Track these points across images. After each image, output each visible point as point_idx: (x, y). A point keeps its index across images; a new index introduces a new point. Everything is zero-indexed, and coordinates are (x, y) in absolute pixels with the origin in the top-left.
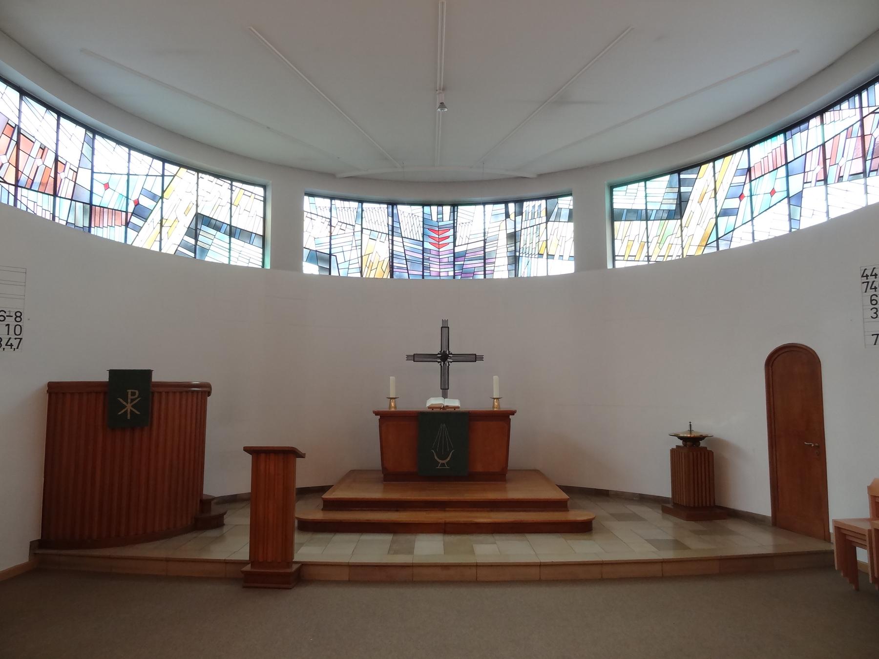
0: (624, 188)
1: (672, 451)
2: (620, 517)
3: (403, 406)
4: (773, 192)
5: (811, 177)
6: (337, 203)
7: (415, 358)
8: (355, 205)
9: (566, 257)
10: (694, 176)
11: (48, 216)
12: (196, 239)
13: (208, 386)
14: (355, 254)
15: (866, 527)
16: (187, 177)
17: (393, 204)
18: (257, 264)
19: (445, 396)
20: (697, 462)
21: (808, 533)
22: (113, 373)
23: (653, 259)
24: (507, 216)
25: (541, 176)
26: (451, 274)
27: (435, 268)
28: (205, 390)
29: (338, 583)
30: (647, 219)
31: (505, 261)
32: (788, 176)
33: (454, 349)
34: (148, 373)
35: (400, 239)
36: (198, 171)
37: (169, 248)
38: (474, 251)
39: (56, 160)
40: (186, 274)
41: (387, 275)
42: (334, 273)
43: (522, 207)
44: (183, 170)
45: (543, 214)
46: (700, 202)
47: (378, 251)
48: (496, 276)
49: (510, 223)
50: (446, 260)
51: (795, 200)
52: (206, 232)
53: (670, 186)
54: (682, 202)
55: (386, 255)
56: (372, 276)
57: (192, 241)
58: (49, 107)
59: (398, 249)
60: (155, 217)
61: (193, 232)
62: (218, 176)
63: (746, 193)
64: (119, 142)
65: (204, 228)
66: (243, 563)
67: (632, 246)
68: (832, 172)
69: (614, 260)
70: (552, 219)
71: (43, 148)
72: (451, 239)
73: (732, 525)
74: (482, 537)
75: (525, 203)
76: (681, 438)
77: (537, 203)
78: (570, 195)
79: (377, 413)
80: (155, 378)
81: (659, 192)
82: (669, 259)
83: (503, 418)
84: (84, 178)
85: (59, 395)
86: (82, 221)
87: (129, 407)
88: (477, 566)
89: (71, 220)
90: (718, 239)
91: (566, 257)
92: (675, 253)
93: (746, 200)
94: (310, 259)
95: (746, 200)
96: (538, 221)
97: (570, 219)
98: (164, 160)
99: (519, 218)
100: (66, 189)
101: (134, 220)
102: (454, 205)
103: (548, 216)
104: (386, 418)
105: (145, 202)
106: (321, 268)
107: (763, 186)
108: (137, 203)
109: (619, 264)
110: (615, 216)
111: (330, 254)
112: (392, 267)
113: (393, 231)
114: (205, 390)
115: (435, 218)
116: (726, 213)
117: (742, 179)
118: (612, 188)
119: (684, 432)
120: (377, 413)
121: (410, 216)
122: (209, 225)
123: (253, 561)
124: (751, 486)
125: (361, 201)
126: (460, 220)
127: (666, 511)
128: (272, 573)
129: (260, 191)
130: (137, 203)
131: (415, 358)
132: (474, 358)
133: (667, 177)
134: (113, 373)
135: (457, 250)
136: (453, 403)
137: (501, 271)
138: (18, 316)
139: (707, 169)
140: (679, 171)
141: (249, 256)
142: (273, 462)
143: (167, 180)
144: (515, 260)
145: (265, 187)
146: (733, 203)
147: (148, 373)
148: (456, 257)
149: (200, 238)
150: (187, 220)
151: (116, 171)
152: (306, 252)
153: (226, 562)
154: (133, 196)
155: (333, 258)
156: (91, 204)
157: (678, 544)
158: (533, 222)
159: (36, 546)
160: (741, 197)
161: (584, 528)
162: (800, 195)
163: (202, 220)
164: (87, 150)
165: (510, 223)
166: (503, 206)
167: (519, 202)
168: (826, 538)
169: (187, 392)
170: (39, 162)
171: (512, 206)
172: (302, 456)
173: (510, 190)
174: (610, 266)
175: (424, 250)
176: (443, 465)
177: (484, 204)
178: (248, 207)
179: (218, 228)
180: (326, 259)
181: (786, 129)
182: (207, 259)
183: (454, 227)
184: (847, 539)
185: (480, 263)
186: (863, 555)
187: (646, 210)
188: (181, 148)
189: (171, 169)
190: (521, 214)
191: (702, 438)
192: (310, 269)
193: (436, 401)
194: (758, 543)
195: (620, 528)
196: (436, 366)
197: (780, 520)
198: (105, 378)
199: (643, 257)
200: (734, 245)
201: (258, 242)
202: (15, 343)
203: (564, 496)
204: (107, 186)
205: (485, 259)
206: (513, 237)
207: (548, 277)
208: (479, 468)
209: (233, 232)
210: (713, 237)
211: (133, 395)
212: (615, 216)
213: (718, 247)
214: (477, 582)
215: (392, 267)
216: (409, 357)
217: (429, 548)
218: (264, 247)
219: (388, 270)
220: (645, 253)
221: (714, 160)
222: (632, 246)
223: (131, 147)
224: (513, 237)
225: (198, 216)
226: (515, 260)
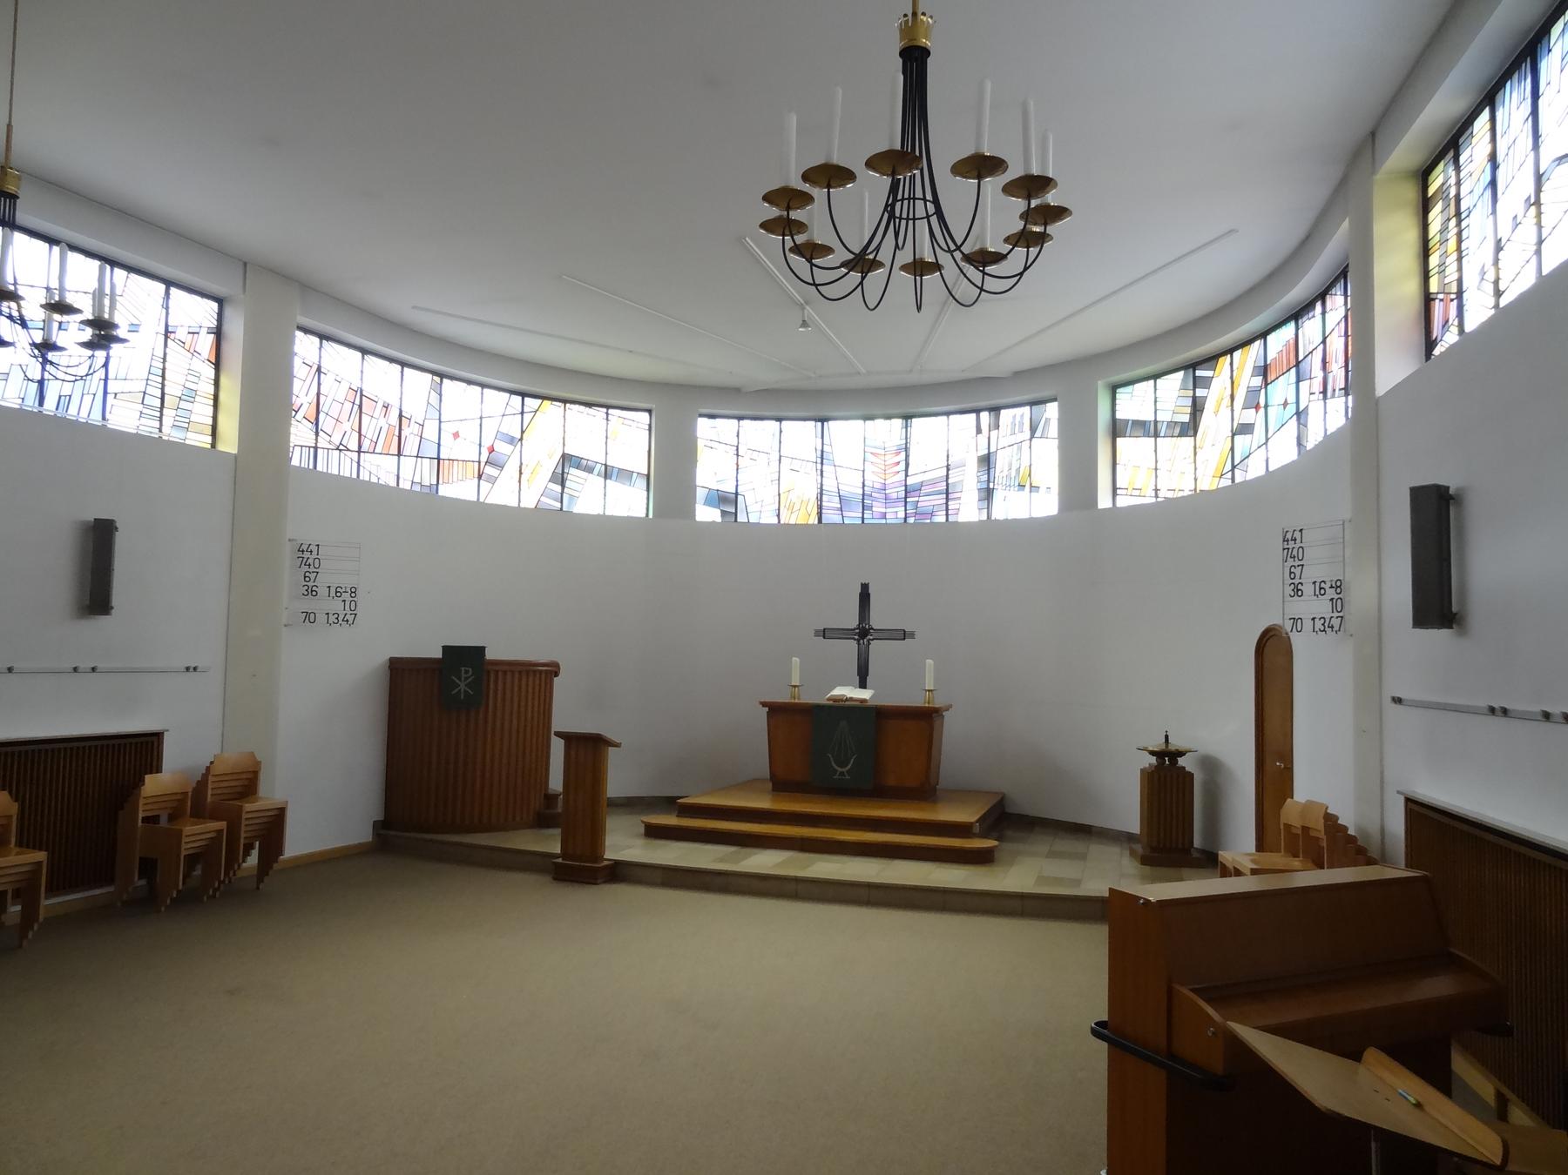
0: (1129, 389)
2: (1052, 855)
3: (808, 698)
4: (1285, 404)
6: (744, 423)
7: (825, 633)
8: (774, 424)
10: (1208, 373)
11: (393, 483)
12: (563, 486)
13: (557, 665)
16: (551, 410)
18: (643, 515)
22: (446, 649)
23: (1161, 494)
24: (979, 431)
25: (1018, 375)
26: (901, 514)
27: (878, 508)
28: (553, 670)
30: (1156, 435)
31: (975, 495)
32: (1298, 381)
34: (481, 650)
36: (565, 401)
37: (529, 502)
38: (934, 482)
39: (401, 416)
40: (551, 530)
41: (813, 520)
42: (742, 518)
44: (547, 403)
48: (962, 518)
49: (983, 438)
50: (894, 496)
51: (1300, 415)
52: (574, 474)
53: (1184, 387)
54: (1197, 408)
56: (792, 522)
57: (558, 488)
58: (391, 360)
59: (829, 485)
61: (560, 479)
63: (1262, 403)
64: (470, 382)
65: (573, 471)
66: (556, 856)
69: (1114, 494)
70: (1038, 434)
71: (386, 407)
72: (902, 466)
76: (1152, 753)
78: (1055, 400)
79: (764, 704)
80: (489, 655)
81: (1170, 393)
82: (1181, 494)
83: (926, 718)
84: (431, 432)
85: (399, 670)
86: (428, 478)
87: (462, 686)
89: (417, 480)
90: (1234, 467)
92: (1184, 487)
94: (708, 502)
95: (1262, 411)
96: (1020, 437)
98: (523, 395)
100: (410, 447)
101: (489, 470)
102: (907, 417)
103: (1033, 430)
104: (775, 711)
105: (502, 448)
106: (724, 513)
108: (491, 450)
109: (1122, 502)
111: (737, 494)
112: (820, 507)
114: (553, 670)
116: (1246, 429)
118: (1114, 389)
119: (1157, 743)
120: (764, 704)
122: (578, 467)
123: (564, 855)
125: (780, 420)
128: (583, 868)
130: (491, 450)
131: (825, 633)
132: (904, 635)
133: (1182, 373)
134: (446, 649)
136: (865, 694)
137: (968, 510)
138: (354, 591)
139: (1224, 361)
140: (1192, 366)
141: (631, 502)
142: (588, 750)
143: (527, 417)
144: (987, 494)
145: (650, 411)
146: (1249, 416)
147: (481, 650)
148: (908, 491)
149: (568, 484)
151: (471, 412)
152: (701, 494)
154: (486, 443)
155: (740, 498)
156: (439, 459)
158: (1013, 439)
159: (378, 826)
160: (1257, 407)
161: (982, 858)
164: (434, 397)
165: (983, 438)
166: (973, 416)
167: (995, 410)
169: (528, 672)
170: (382, 422)
171: (985, 416)
172: (617, 745)
173: (977, 394)
174: (1104, 502)
176: (842, 774)
177: (948, 414)
178: (627, 437)
179: (590, 470)
180: (727, 501)
181: (1297, 314)
182: (576, 510)
183: (906, 449)
185: (941, 499)
187: (1156, 422)
188: (539, 381)
189: (531, 403)
190: (997, 427)
191: (1181, 754)
192: (706, 514)
196: (852, 645)
198: (439, 655)
200: (1251, 476)
202: (351, 618)
204: (456, 435)
205: (947, 493)
206: (987, 461)
207: (1032, 520)
208: (891, 781)
209: (607, 473)
210: (1228, 466)
211: (467, 673)
212: (1117, 429)
213: (1233, 479)
215: (820, 507)
216: (817, 633)
219: (815, 511)
221: (1230, 351)
222: (1146, 473)
223: (483, 386)
224: (987, 461)
225: (566, 458)
226: (987, 494)
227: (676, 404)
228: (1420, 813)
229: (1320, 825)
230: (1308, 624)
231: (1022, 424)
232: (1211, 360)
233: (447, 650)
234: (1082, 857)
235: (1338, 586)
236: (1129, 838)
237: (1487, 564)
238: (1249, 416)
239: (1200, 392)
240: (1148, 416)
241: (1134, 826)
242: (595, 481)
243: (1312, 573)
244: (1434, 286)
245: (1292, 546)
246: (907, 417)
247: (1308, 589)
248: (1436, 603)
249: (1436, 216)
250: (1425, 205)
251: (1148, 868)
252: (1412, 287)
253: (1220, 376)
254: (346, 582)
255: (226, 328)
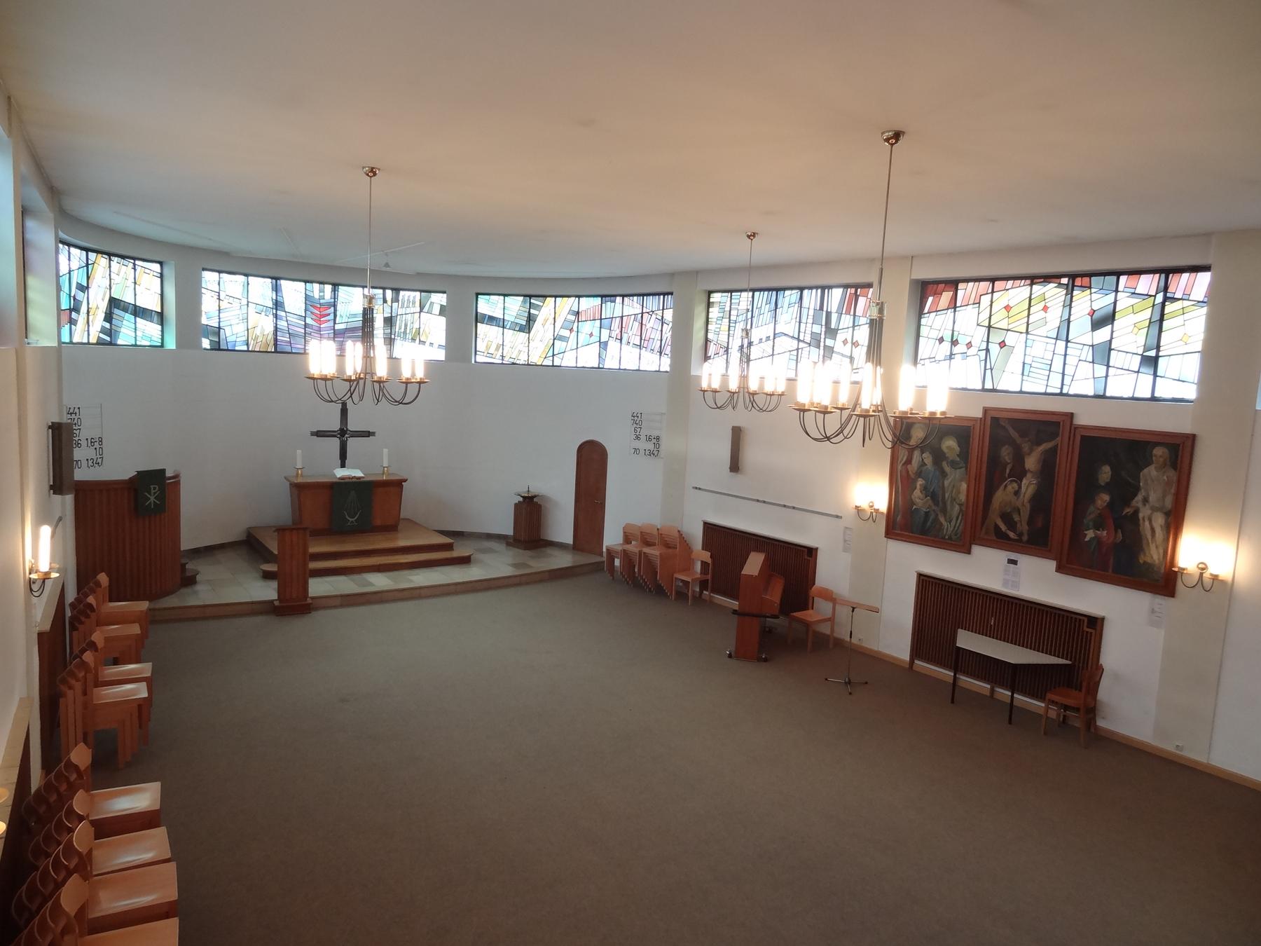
1: (516, 505)
2: (485, 551)
4: (591, 335)
5: (614, 334)
7: (319, 434)
9: (436, 345)
14: (242, 327)
15: (620, 548)
17: (277, 279)
19: (343, 465)
20: (530, 511)
21: (591, 552)
24: (385, 301)
25: (418, 274)
29: (335, 607)
33: (352, 426)
34: (163, 471)
35: (283, 314)
43: (398, 295)
45: (418, 304)
46: (543, 325)
47: (264, 326)
51: (603, 345)
54: (531, 319)
55: (272, 329)
57: (107, 325)
59: (282, 324)
60: (84, 309)
62: (123, 257)
63: (575, 328)
65: (116, 311)
66: (272, 602)
67: (490, 344)
68: (625, 337)
70: (426, 309)
72: (331, 317)
73: (549, 551)
74: (417, 571)
75: (402, 293)
77: (412, 294)
81: (514, 307)
83: (398, 484)
87: (152, 499)
88: (421, 588)
91: (436, 345)
92: (522, 359)
93: (574, 334)
95: (574, 334)
96: (412, 310)
97: (440, 314)
99: (395, 305)
101: (74, 315)
102: (335, 286)
105: (80, 296)
107: (587, 327)
109: (480, 359)
110: (479, 318)
111: (219, 328)
112: (276, 340)
113: (278, 305)
115: (317, 296)
116: (561, 338)
117: (573, 318)
118: (477, 294)
119: (523, 490)
121: (294, 293)
124: (562, 527)
125: (246, 275)
126: (340, 299)
127: (508, 544)
128: (294, 604)
129: (156, 267)
131: (319, 434)
132: (368, 434)
135: (337, 327)
139: (550, 301)
140: (530, 296)
145: (161, 263)
146: (565, 333)
147: (163, 471)
150: (104, 305)
153: (252, 603)
157: (515, 566)
160: (571, 330)
161: (465, 561)
162: (606, 343)
163: (114, 303)
166: (381, 291)
167: (396, 290)
168: (601, 554)
171: (389, 292)
175: (306, 326)
179: (125, 310)
183: (335, 306)
184: (611, 554)
186: (617, 562)
189: (92, 256)
190: (397, 301)
193: (340, 473)
194: (563, 560)
195: (485, 557)
197: (577, 547)
199: (498, 356)
201: (156, 318)
203: (447, 540)
208: (378, 522)
209: (138, 312)
210: (550, 354)
211: (154, 489)
214: (420, 597)
215: (276, 340)
216: (313, 434)
217: (380, 582)
218: (162, 325)
220: (500, 353)
221: (556, 297)
222: (490, 344)
227: (187, 261)
228: (709, 528)
229: (676, 535)
230: (642, 452)
231: (414, 303)
232: (545, 297)
233: (141, 474)
234: (490, 551)
235: (658, 438)
236: (489, 537)
237: (752, 455)
238: (565, 333)
239: (532, 311)
240: (498, 314)
241: (508, 530)
242: (129, 317)
243: (644, 433)
244: (710, 336)
245: (636, 419)
246: (335, 286)
247: (643, 438)
248: (735, 466)
249: (714, 313)
250: (709, 305)
251: (528, 553)
252: (702, 333)
253: (546, 309)
254: (96, 435)
255: (28, 236)
